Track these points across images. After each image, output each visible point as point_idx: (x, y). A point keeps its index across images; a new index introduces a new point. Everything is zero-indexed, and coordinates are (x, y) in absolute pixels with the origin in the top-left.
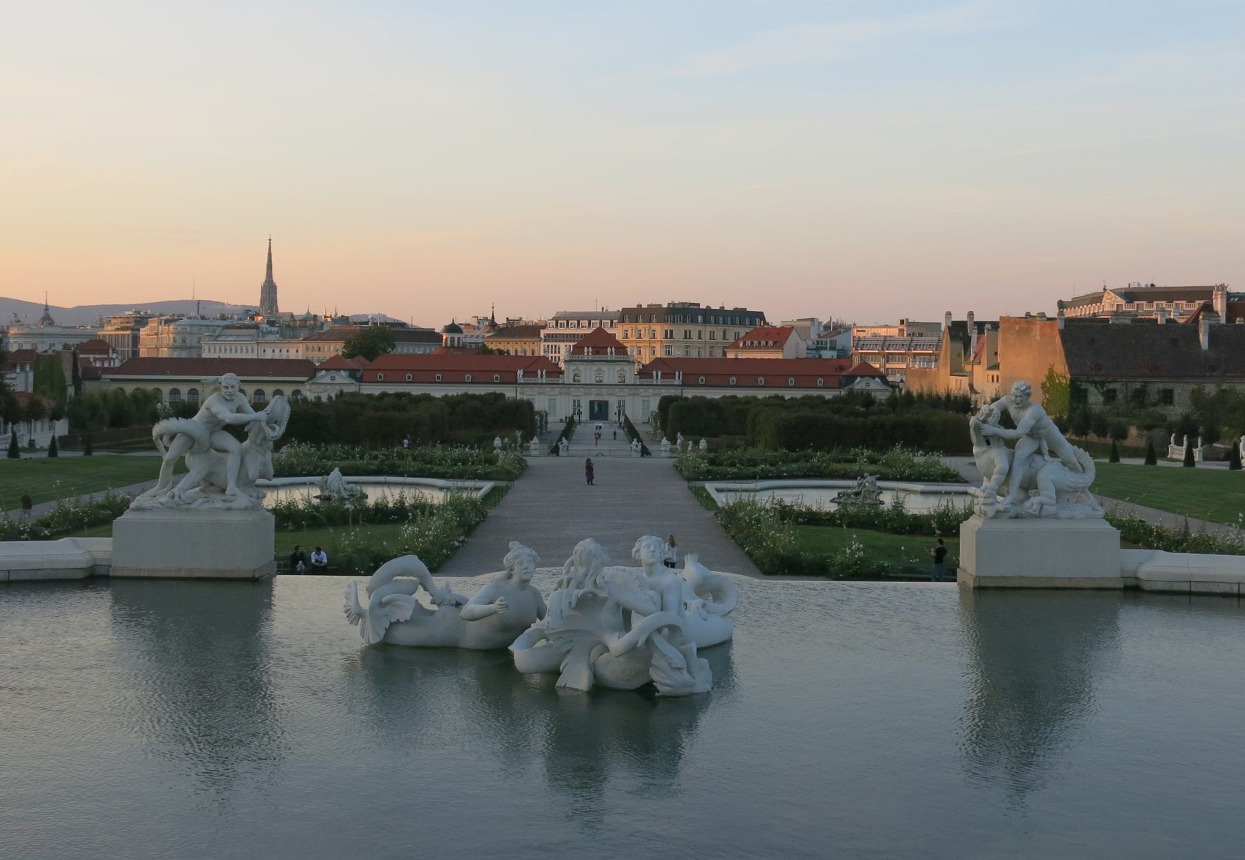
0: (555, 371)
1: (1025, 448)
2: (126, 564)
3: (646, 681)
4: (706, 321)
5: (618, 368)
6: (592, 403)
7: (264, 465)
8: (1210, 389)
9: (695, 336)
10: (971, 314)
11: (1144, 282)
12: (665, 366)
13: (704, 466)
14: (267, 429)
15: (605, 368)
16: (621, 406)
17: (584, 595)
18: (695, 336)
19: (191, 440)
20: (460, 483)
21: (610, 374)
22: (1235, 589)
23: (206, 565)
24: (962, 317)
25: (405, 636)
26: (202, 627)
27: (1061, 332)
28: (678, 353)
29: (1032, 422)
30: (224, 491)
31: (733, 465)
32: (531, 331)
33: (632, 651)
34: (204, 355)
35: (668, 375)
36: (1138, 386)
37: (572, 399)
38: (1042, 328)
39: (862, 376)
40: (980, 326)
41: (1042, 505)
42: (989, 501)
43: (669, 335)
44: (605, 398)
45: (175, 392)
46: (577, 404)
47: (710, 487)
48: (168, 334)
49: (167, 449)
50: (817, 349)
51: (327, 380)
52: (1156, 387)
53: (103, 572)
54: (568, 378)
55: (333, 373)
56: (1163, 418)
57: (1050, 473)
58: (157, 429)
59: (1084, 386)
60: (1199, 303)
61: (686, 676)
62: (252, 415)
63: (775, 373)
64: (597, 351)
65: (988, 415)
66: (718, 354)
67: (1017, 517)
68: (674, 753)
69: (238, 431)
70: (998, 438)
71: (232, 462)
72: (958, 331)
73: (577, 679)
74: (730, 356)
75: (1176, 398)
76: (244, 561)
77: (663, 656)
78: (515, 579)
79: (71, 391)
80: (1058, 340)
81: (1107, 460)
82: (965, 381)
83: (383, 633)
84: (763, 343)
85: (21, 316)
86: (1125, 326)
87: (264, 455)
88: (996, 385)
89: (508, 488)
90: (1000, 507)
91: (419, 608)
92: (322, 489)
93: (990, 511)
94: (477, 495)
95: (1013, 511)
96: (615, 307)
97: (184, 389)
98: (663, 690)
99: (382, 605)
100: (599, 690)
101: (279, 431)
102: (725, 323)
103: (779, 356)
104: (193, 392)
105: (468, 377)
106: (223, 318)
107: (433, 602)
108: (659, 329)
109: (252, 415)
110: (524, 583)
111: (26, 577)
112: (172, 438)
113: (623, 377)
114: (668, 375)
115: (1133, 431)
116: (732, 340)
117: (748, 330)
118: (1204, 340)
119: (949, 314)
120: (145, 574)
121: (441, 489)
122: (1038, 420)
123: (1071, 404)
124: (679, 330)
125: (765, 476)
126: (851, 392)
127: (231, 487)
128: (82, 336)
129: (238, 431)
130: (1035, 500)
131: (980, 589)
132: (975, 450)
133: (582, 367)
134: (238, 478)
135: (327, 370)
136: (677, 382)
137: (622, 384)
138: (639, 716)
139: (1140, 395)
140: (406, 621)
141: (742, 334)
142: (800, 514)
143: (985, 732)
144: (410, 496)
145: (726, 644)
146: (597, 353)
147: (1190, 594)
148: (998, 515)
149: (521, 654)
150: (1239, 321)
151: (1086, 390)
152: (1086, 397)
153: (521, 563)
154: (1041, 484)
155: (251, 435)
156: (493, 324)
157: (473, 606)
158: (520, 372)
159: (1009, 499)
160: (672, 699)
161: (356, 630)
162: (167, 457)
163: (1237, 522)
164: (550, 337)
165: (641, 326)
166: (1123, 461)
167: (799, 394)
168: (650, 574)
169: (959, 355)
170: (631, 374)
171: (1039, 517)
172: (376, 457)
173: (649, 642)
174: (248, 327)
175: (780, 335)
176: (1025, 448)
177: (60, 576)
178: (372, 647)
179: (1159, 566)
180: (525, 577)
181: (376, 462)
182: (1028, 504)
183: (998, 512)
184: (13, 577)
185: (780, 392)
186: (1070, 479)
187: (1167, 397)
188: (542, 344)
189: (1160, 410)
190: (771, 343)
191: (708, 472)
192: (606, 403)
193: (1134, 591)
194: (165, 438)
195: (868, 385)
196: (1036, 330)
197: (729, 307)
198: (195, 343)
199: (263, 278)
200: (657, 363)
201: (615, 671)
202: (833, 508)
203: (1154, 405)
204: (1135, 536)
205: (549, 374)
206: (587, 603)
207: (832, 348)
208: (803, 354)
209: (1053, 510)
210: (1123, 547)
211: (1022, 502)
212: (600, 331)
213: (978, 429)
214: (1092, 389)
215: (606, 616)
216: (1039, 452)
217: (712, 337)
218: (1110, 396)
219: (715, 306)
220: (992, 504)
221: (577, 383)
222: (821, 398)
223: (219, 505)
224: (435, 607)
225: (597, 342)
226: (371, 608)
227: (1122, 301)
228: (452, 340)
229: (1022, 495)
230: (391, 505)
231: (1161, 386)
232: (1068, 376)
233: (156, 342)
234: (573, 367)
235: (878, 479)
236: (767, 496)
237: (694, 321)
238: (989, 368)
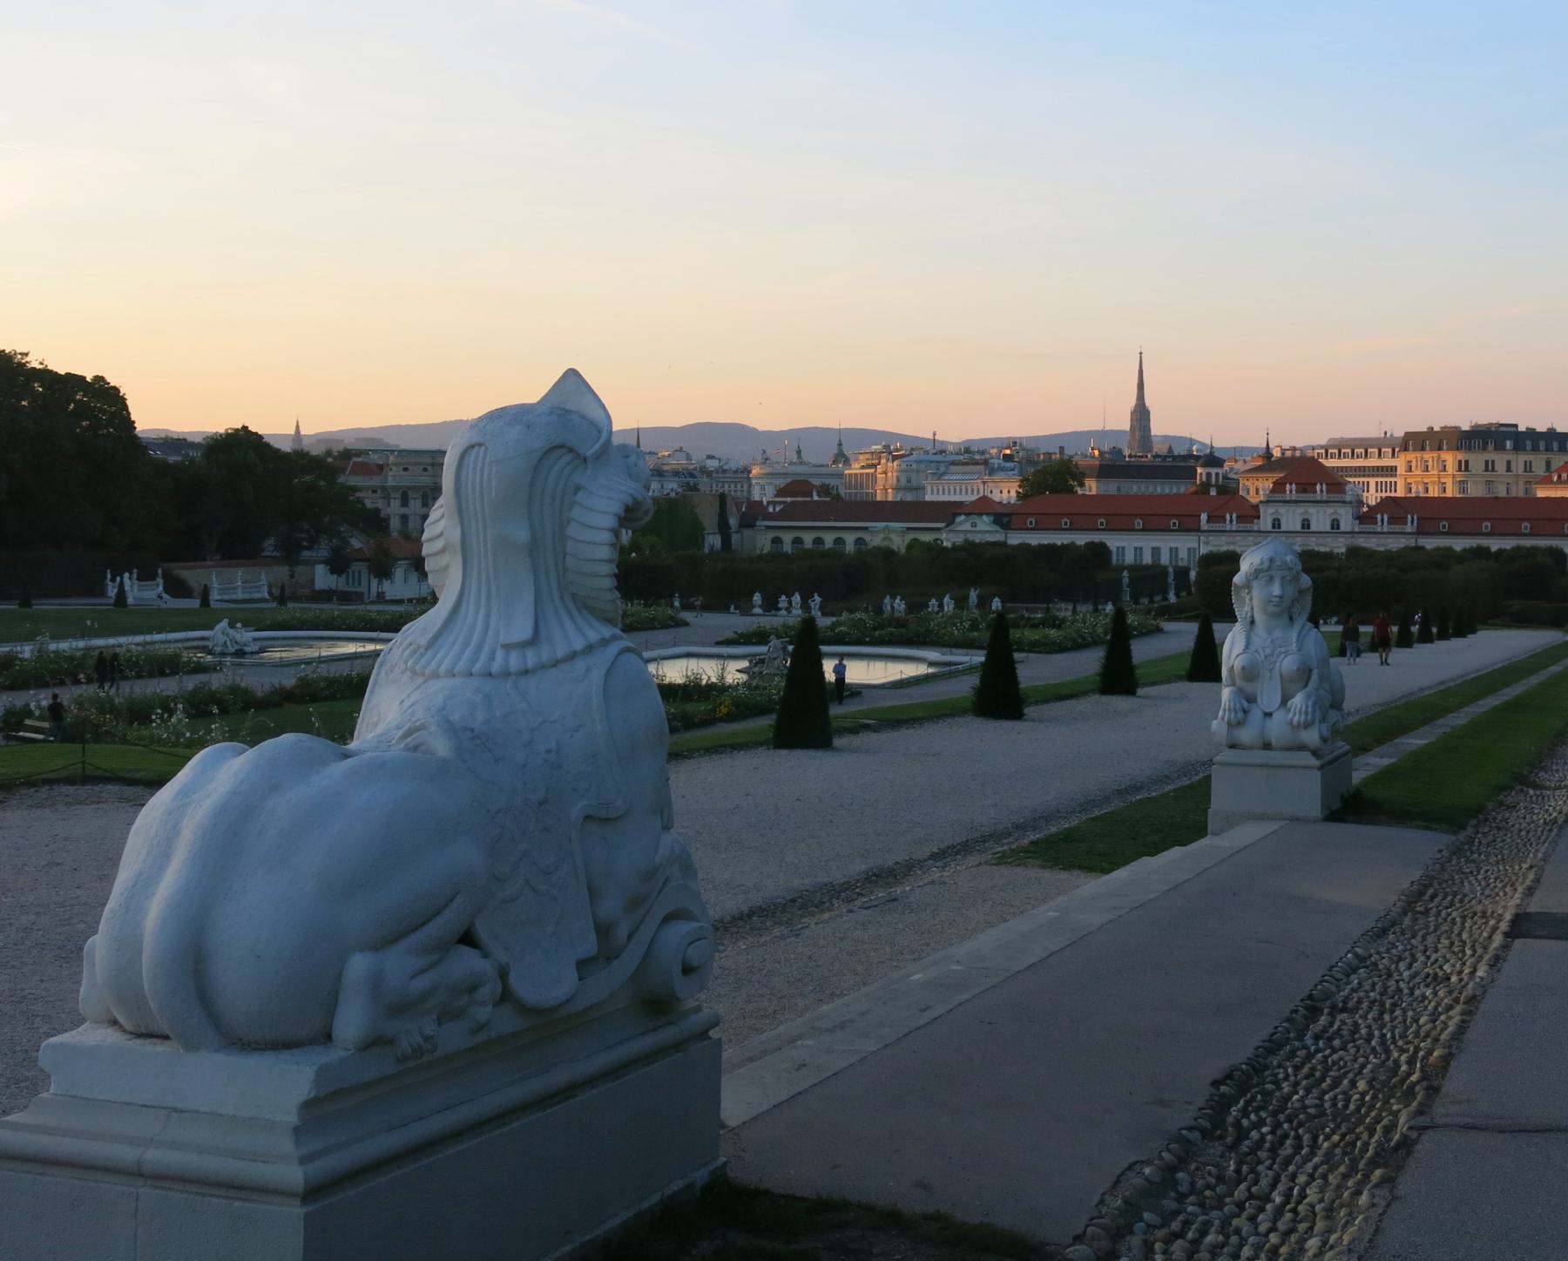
4: (1518, 448)
9: (1500, 467)
18: (1500, 467)
28: (1475, 490)
34: (928, 498)
43: (1464, 466)
51: (967, 526)
54: (1265, 523)
55: (975, 518)
64: (1306, 487)
74: (1541, 493)
79: (713, 540)
85: (771, 453)
102: (1548, 449)
105: (1139, 523)
108: (1450, 458)
113: (1335, 524)
124: (1477, 460)
128: (785, 475)
133: (1282, 510)
135: (968, 514)
136: (1409, 528)
146: (1304, 491)
156: (1268, 453)
158: (1204, 517)
165: (1427, 456)
174: (977, 463)
199: (1133, 401)
205: (1240, 519)
217: (1528, 467)
219: (1541, 428)
228: (1209, 475)
233: (885, 483)
234: (1271, 510)
237: (1499, 447)
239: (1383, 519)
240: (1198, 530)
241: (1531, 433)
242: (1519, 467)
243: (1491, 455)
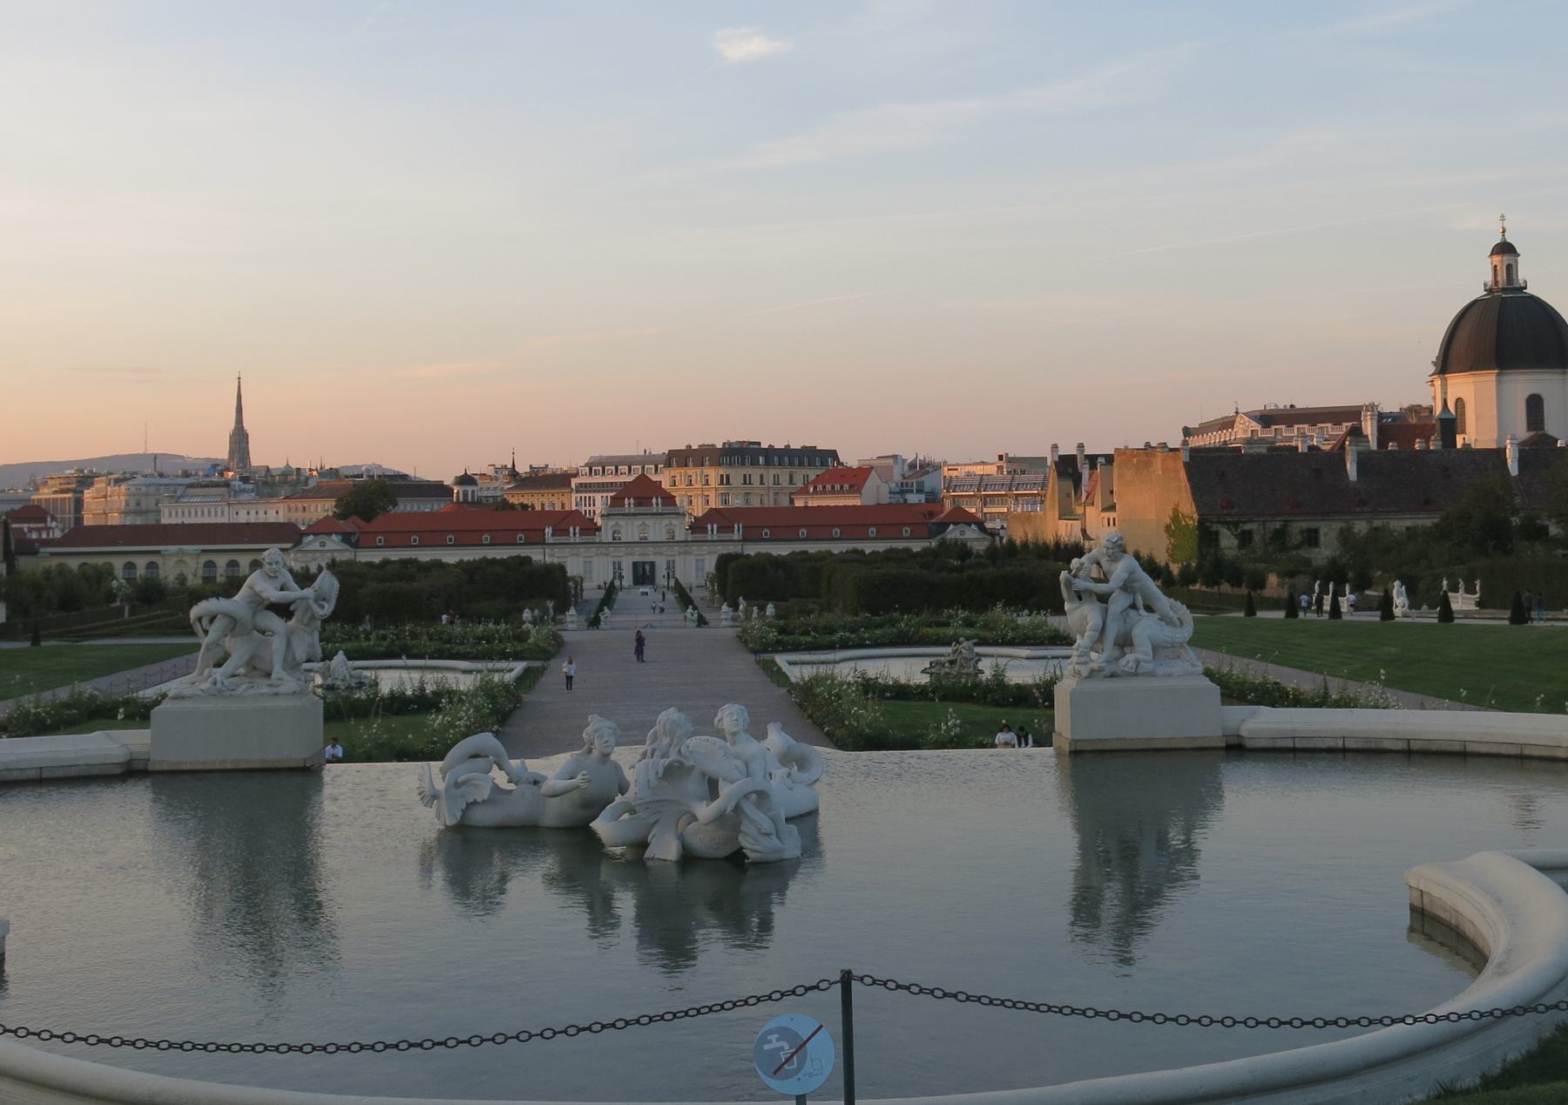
0: (590, 528)
1: (1119, 602)
2: (167, 757)
3: (734, 849)
4: (768, 463)
5: (665, 522)
6: (635, 564)
7: (312, 645)
8: (1361, 527)
9: (756, 480)
10: (1081, 446)
11: (1282, 403)
12: (721, 518)
13: (773, 635)
14: (315, 607)
15: (650, 522)
16: (670, 567)
17: (670, 764)
18: (756, 480)
19: (233, 623)
20: (490, 665)
21: (656, 530)
22: (1340, 744)
23: (253, 756)
24: (1068, 449)
25: (481, 816)
26: (252, 826)
27: (1186, 465)
28: (736, 502)
29: (1125, 576)
30: (269, 675)
31: (806, 633)
32: (560, 480)
33: (720, 819)
34: (163, 521)
35: (726, 528)
36: (1278, 525)
37: (611, 560)
38: (1163, 461)
39: (955, 524)
40: (1092, 459)
41: (1138, 662)
42: (1083, 659)
43: (725, 480)
44: (651, 558)
45: (130, 566)
46: (617, 567)
47: (781, 660)
48: (119, 496)
49: (206, 632)
50: (902, 492)
51: (316, 546)
52: (1298, 526)
53: (141, 766)
54: (606, 535)
55: (323, 538)
56: (1308, 562)
57: (1146, 628)
58: (195, 612)
59: (1214, 528)
60: (1346, 426)
61: (775, 841)
62: (295, 592)
63: (853, 523)
64: (641, 501)
65: (1079, 569)
66: (785, 502)
67: (1112, 676)
68: (766, 926)
69: (283, 610)
70: (1090, 592)
71: (278, 644)
72: (1067, 467)
73: (665, 849)
74: (799, 503)
75: (1322, 539)
76: (291, 752)
77: (753, 822)
78: (595, 753)
80: (1183, 474)
81: (1242, 615)
82: (1077, 524)
83: (459, 814)
84: (837, 487)
86: (1260, 456)
87: (311, 634)
88: (1112, 529)
89: (544, 669)
90: (1095, 666)
91: (496, 787)
92: (324, 676)
93: (1085, 671)
94: (509, 677)
95: (1109, 669)
96: (660, 448)
97: (141, 563)
98: (752, 856)
99: (457, 785)
100: (688, 860)
101: (328, 609)
103: (858, 502)
104: (152, 566)
105: (486, 537)
106: (186, 474)
107: (510, 781)
108: (713, 474)
109: (295, 592)
110: (605, 756)
111: (60, 773)
112: (212, 620)
113: (671, 533)
114: (726, 528)
115: (1273, 579)
116: (800, 485)
117: (819, 472)
118: (1351, 468)
119: (1055, 447)
120: (188, 767)
121: (465, 672)
122: (1132, 573)
123: (1200, 548)
124: (737, 475)
125: (845, 645)
126: (943, 543)
127: (278, 671)
129: (283, 610)
130: (1130, 657)
131: (1076, 753)
132: (1067, 606)
134: (285, 661)
136: (736, 537)
137: (671, 541)
138: (732, 883)
139: (1280, 536)
140: (484, 802)
141: (812, 477)
142: (886, 688)
143: (1085, 908)
144: (431, 681)
145: (813, 813)
147: (1294, 750)
148: (1092, 674)
149: (600, 826)
150: (1392, 446)
151: (1217, 533)
152: (1217, 540)
153: (601, 736)
154: (1136, 641)
155: (297, 615)
156: (513, 474)
157: (554, 782)
158: (548, 530)
159: (1103, 657)
160: (763, 865)
161: (430, 813)
162: (205, 641)
163: (1379, 680)
164: (583, 487)
165: (691, 471)
166: (1261, 614)
167: (881, 547)
168: (734, 743)
169: (1069, 495)
170: (681, 530)
171: (1136, 674)
172: (384, 638)
173: (737, 809)
174: (217, 485)
175: (856, 478)
176: (1119, 602)
177: (95, 772)
178: (448, 828)
179: (1263, 722)
180: (607, 751)
181: (385, 643)
182: (1123, 662)
183: (1092, 670)
184: (46, 775)
185: (859, 546)
186: (1166, 633)
187: (1312, 538)
188: (574, 495)
189: (1304, 553)
190: (846, 486)
191: (778, 642)
192: (652, 564)
193: (1237, 749)
194: (205, 621)
195: (962, 533)
196: (1157, 463)
197: (795, 445)
198: (152, 506)
199: (232, 425)
200: (713, 515)
201: (704, 840)
202: (925, 679)
203: (1298, 547)
204: (1235, 692)
206: (674, 772)
207: (919, 491)
208: (885, 499)
209: (1150, 667)
210: (1223, 703)
211: (1117, 659)
212: (643, 478)
213: (1069, 584)
214: (1224, 531)
215: (693, 785)
216: (1134, 606)
218: (1245, 539)
219: (779, 445)
220: (1086, 663)
221: (616, 542)
222: (907, 550)
223: (265, 690)
224: (512, 786)
225: (640, 493)
226: (447, 789)
227: (1258, 427)
228: (465, 494)
229: (1117, 653)
230: (409, 692)
231: (1305, 525)
232: (1196, 516)
234: (611, 523)
235: (976, 644)
236: (847, 668)
237: (755, 463)
238: (1104, 510)
239: (712, 531)
240: (543, 543)
241: (787, 450)
242: (769, 481)
243: (749, 470)
